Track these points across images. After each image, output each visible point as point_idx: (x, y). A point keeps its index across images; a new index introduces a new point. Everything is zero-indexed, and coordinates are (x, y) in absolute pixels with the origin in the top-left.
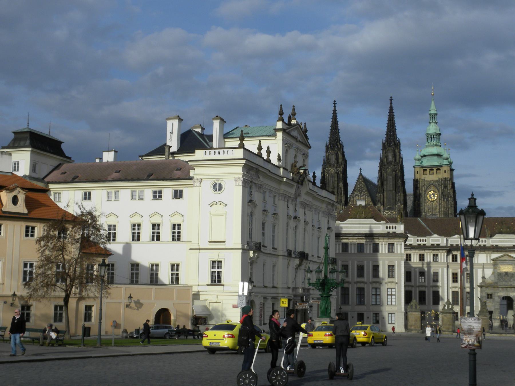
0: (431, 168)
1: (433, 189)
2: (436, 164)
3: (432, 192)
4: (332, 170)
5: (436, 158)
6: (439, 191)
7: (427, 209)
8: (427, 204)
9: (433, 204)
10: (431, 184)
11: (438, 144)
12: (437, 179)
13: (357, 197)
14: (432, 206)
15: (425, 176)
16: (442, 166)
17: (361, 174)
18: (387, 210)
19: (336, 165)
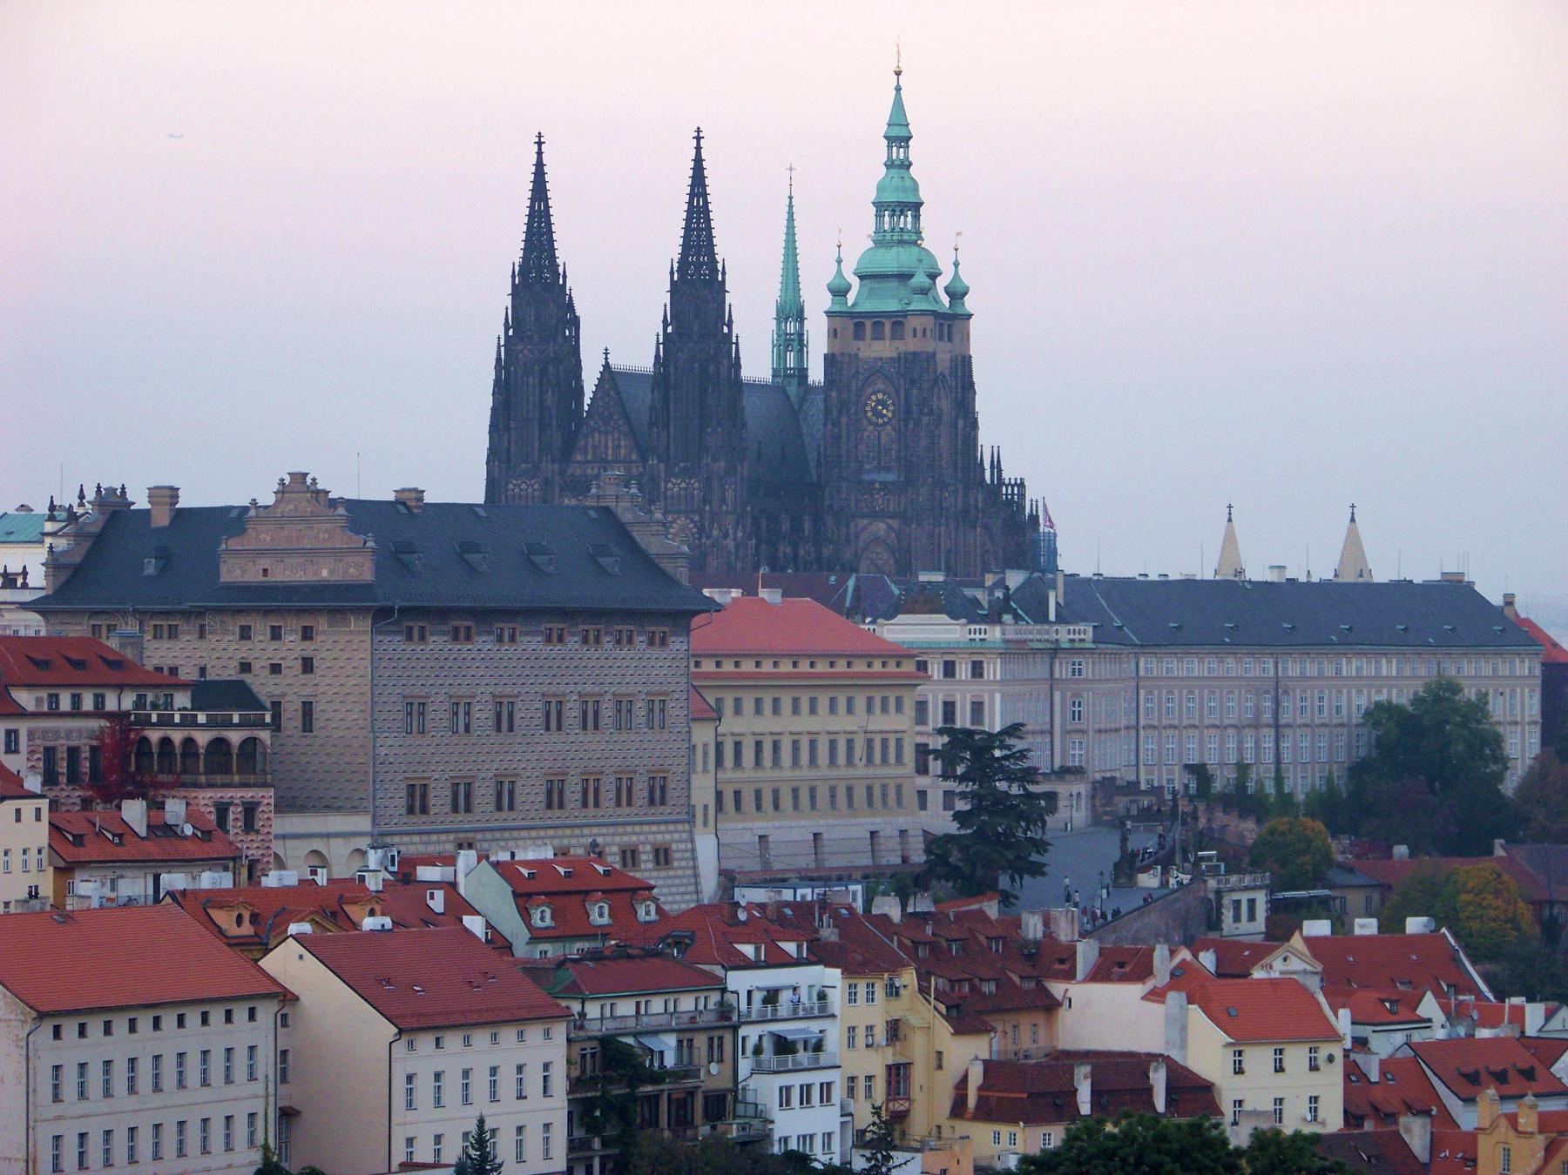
0: (878, 318)
1: (883, 387)
2: (892, 305)
3: (880, 396)
4: (526, 351)
5: (894, 284)
6: (898, 393)
7: (862, 447)
8: (866, 434)
9: (883, 434)
10: (877, 369)
11: (906, 237)
12: (894, 355)
13: (596, 436)
14: (879, 440)
15: (861, 344)
16: (904, 314)
17: (607, 366)
18: (677, 477)
19: (536, 339)
